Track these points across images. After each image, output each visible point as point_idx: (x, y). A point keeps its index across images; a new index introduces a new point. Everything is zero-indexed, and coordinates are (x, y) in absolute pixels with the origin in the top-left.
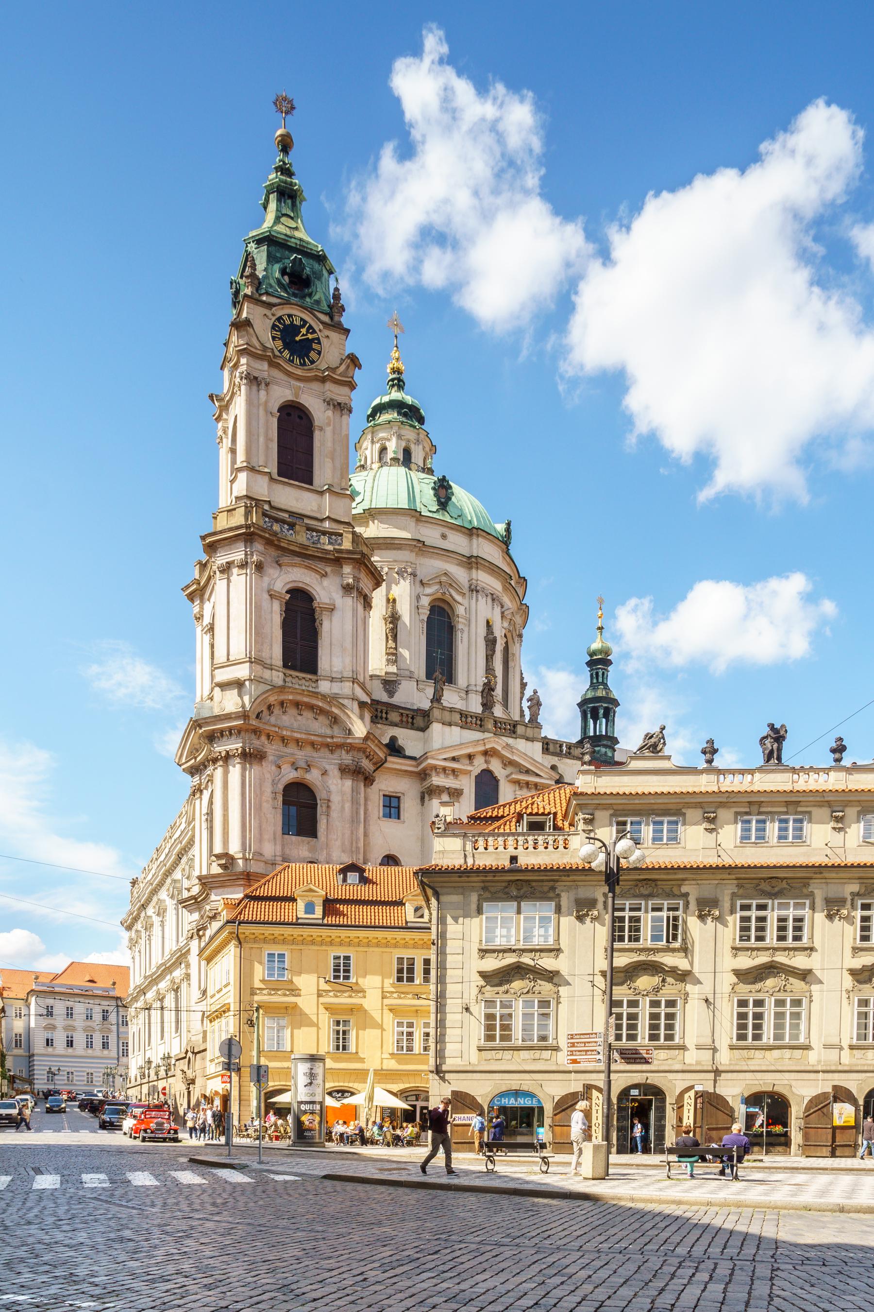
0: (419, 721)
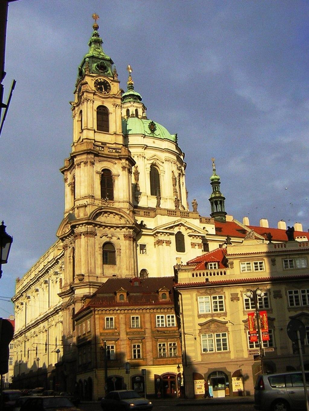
0: (152, 214)
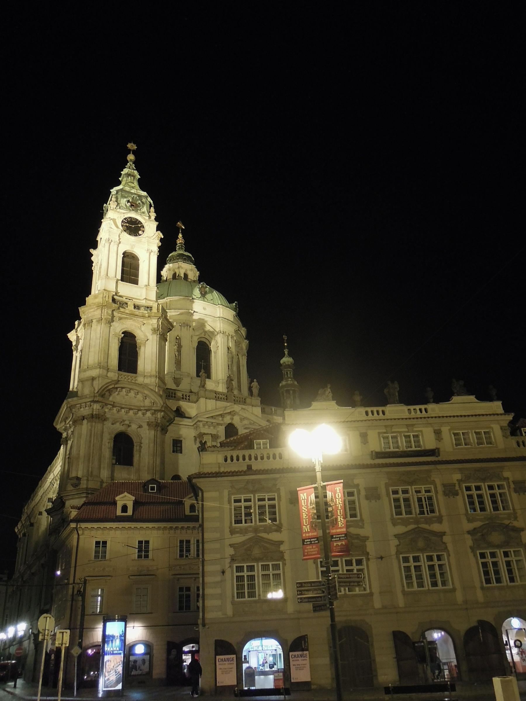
0: (193, 397)
